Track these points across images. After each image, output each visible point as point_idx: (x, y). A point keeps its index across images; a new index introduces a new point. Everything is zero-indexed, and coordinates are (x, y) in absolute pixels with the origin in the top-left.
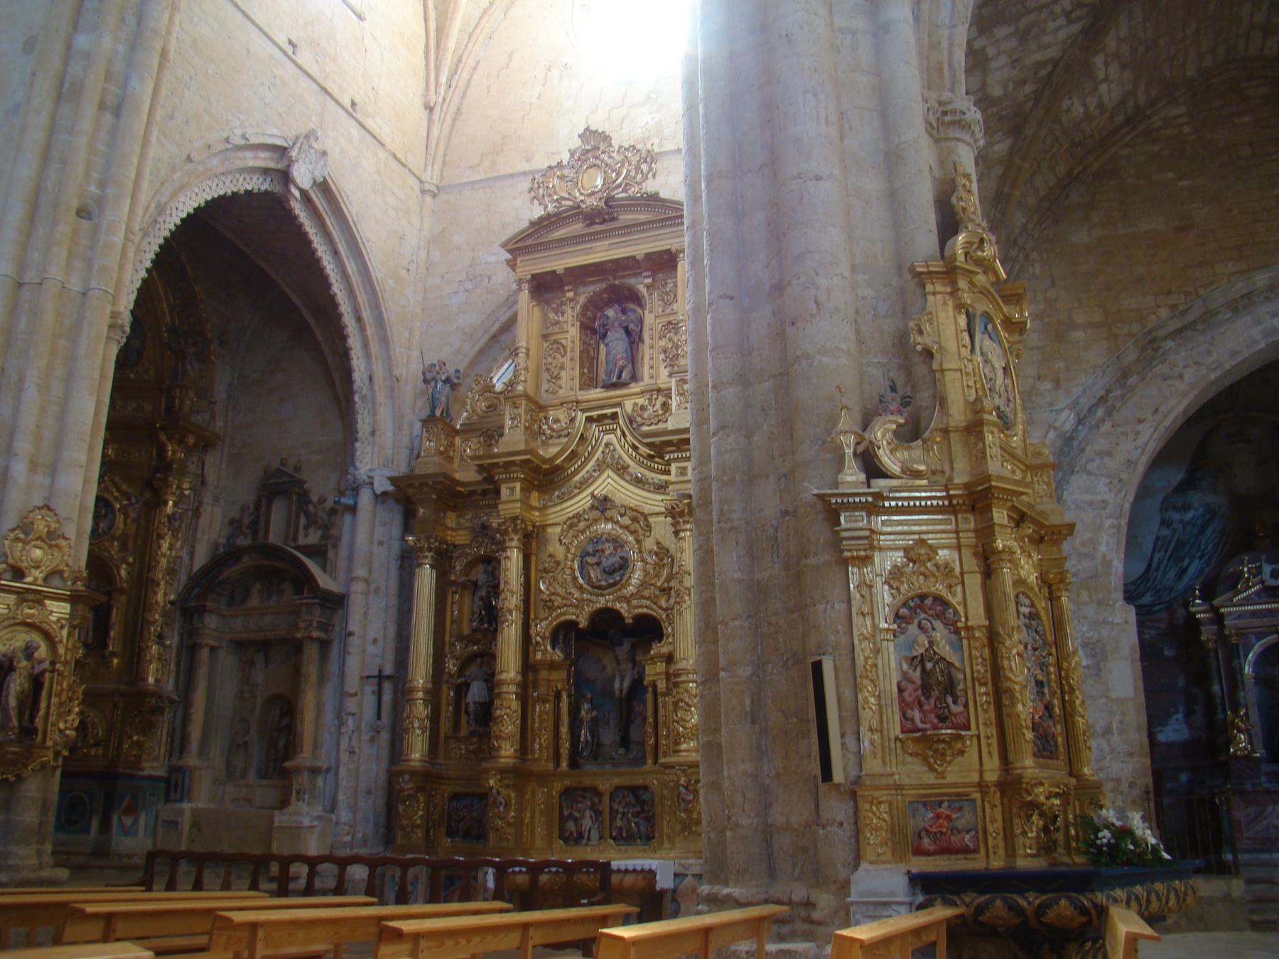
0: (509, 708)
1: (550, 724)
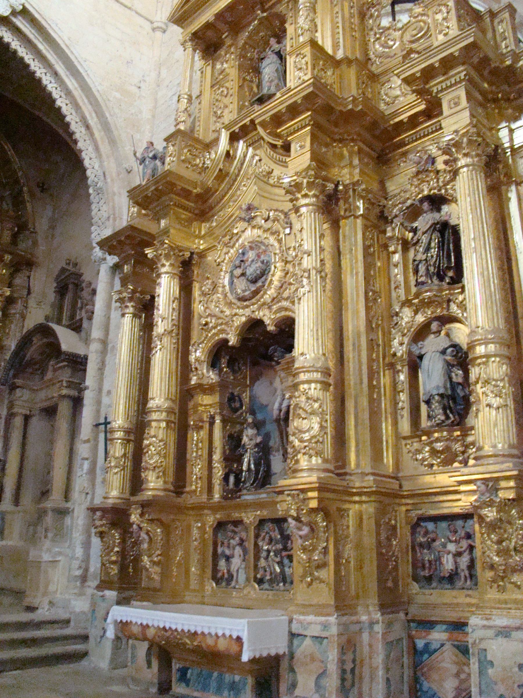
0: (154, 436)
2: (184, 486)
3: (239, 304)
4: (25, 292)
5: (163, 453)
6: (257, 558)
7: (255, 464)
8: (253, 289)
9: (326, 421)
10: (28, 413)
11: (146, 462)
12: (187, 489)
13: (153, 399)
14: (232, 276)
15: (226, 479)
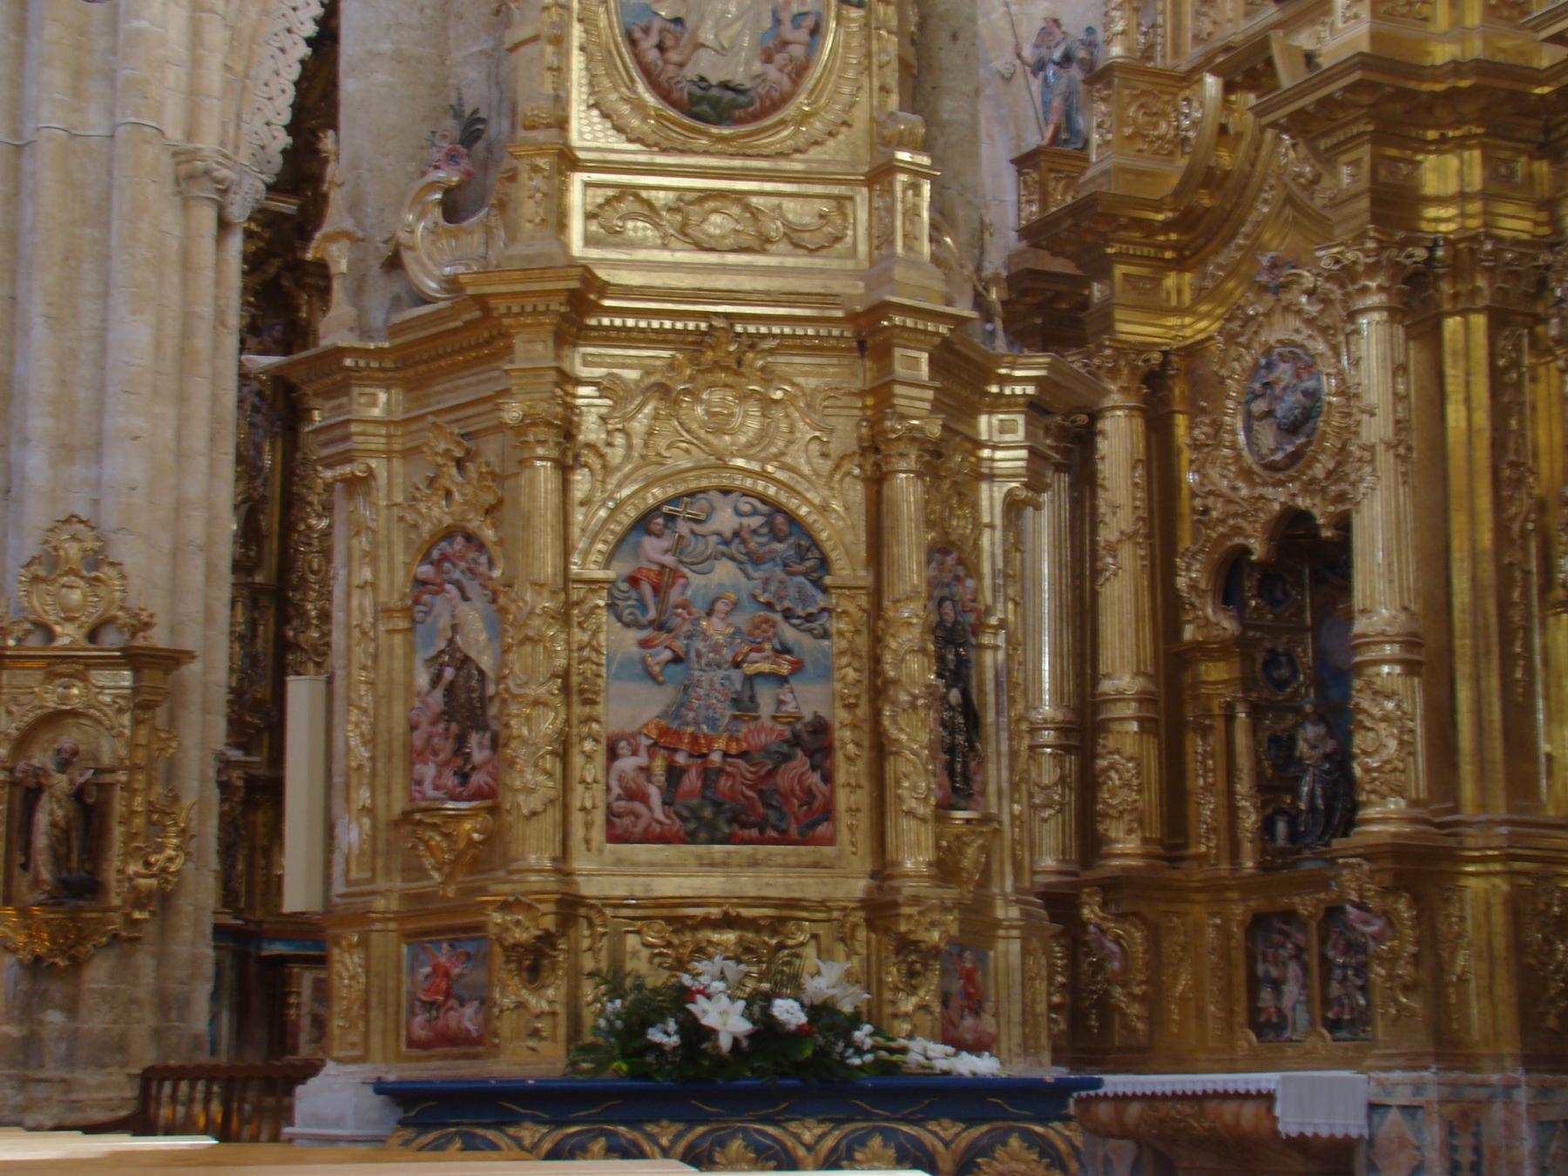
0: (1117, 752)
1: (1219, 778)
2: (1185, 846)
3: (1265, 474)
5: (1135, 782)
6: (1325, 981)
7: (1324, 797)
8: (1290, 448)
9: (1412, 731)
11: (1105, 802)
12: (1192, 851)
13: (1107, 676)
14: (1249, 417)
15: (1267, 826)
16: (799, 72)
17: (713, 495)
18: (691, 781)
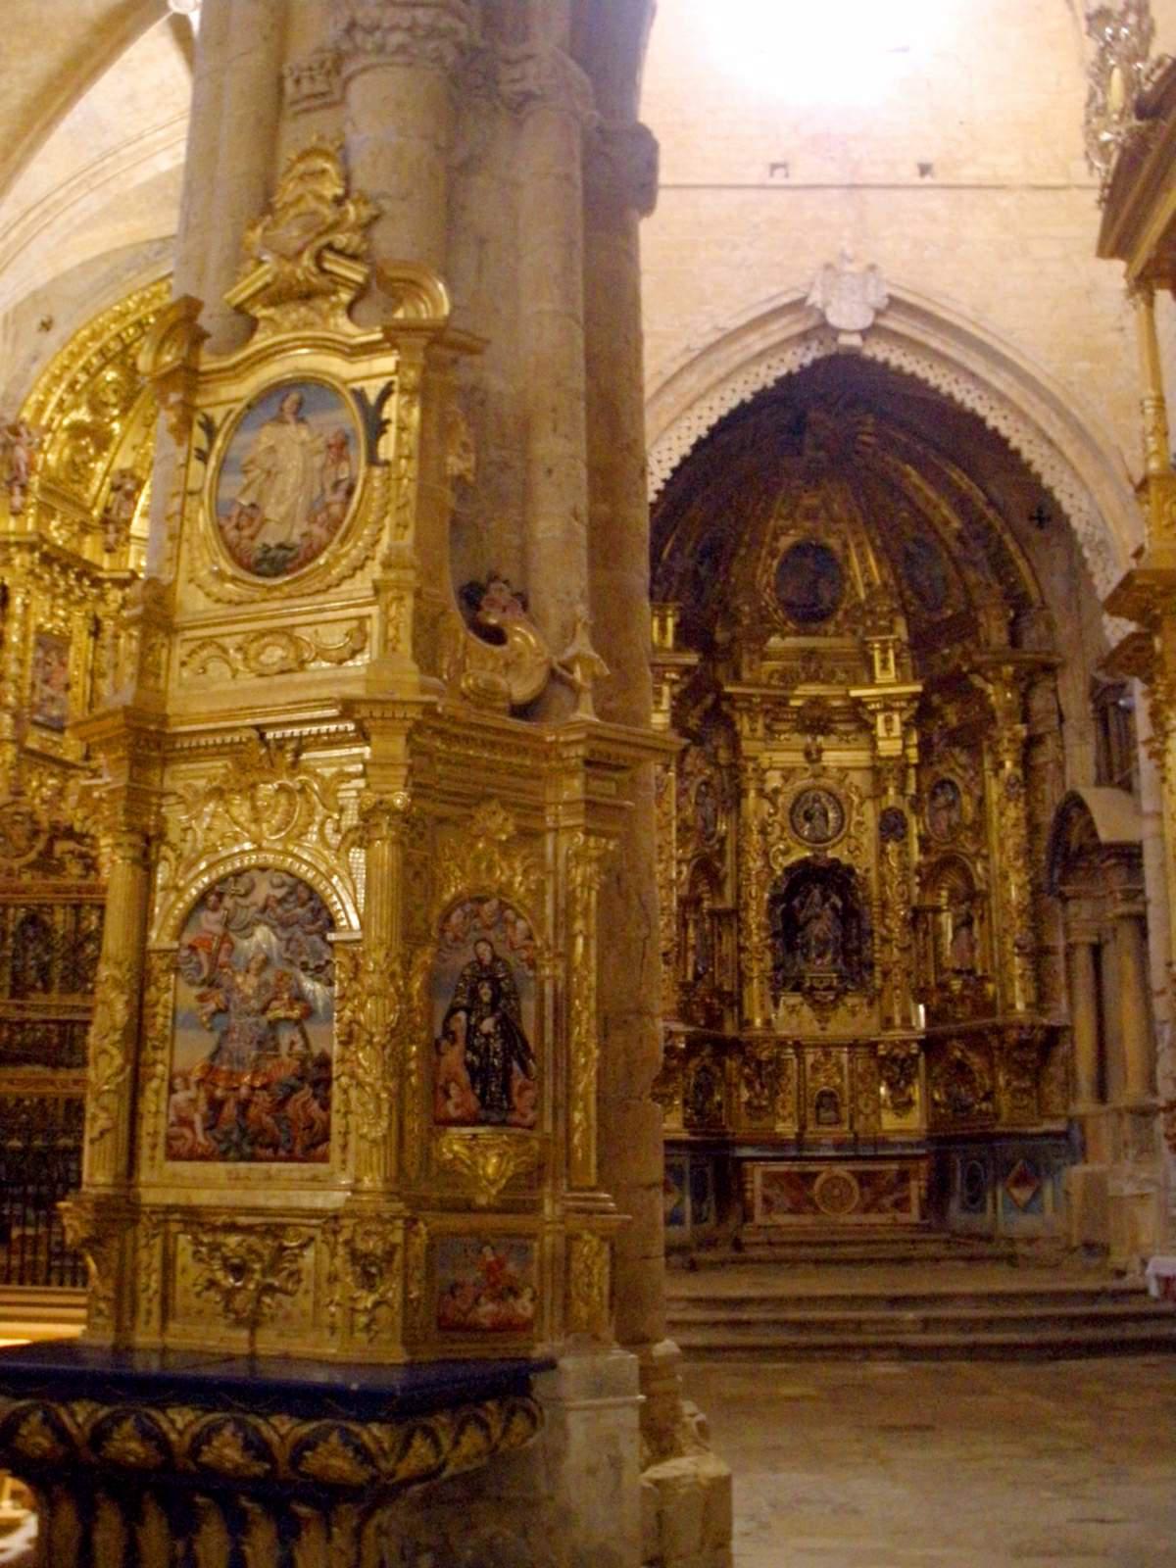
4: (1054, 720)
10: (1095, 939)
16: (333, 525)
17: (255, 874)
18: (230, 1110)
